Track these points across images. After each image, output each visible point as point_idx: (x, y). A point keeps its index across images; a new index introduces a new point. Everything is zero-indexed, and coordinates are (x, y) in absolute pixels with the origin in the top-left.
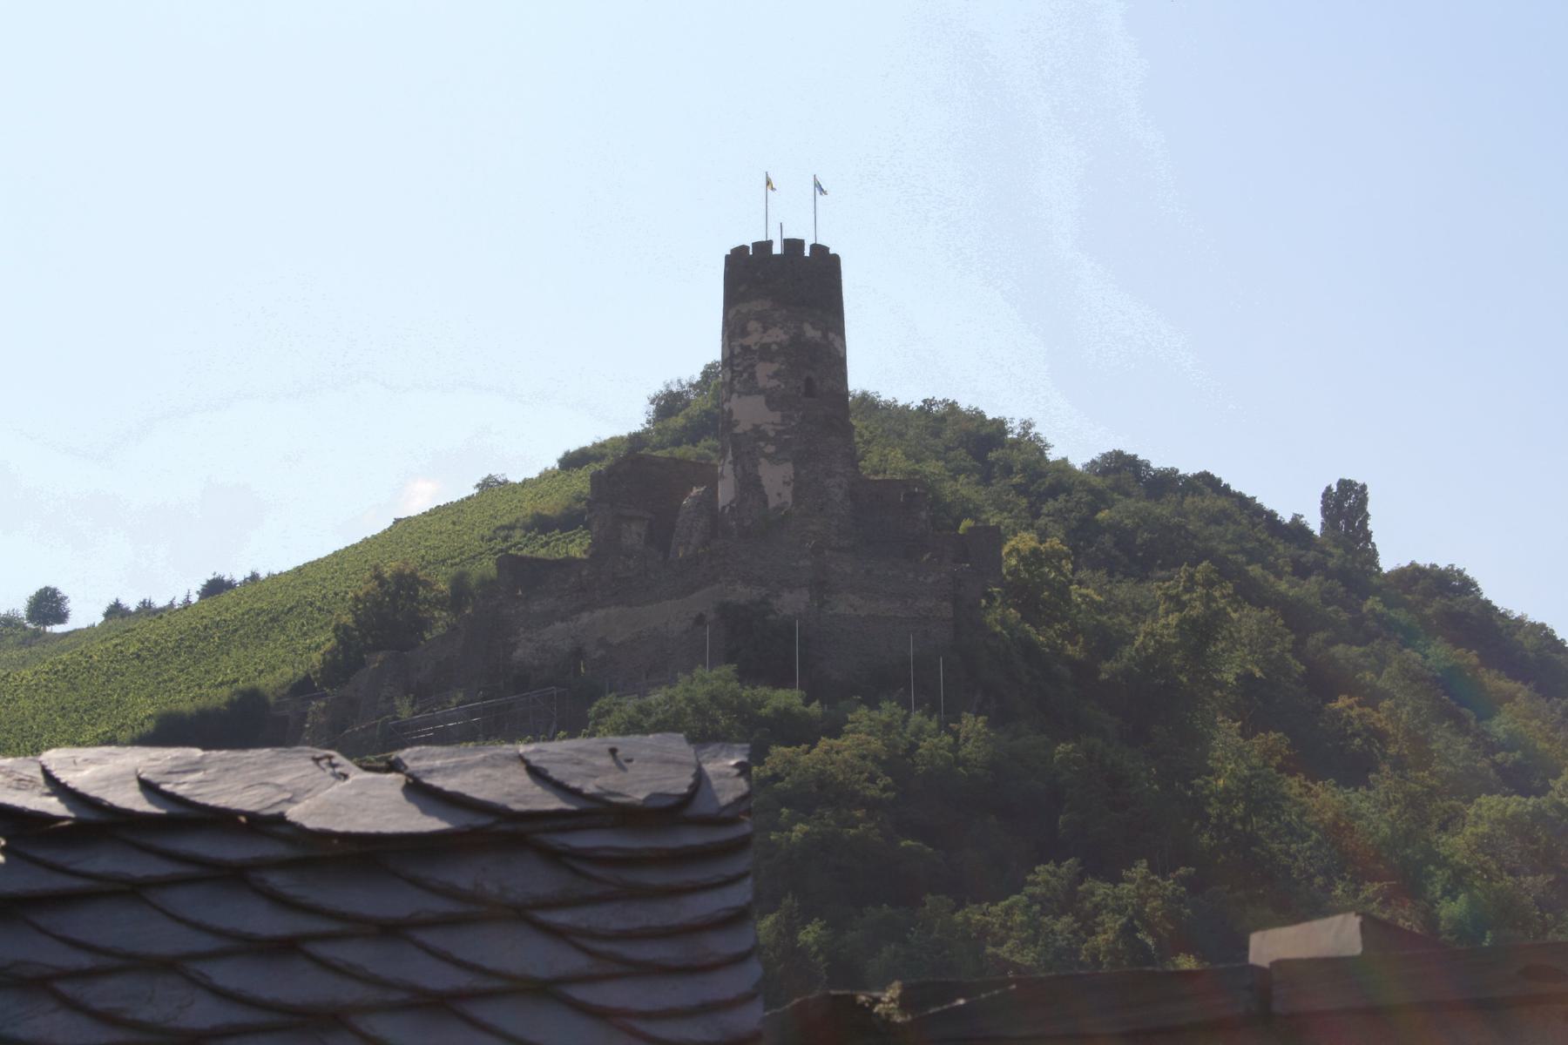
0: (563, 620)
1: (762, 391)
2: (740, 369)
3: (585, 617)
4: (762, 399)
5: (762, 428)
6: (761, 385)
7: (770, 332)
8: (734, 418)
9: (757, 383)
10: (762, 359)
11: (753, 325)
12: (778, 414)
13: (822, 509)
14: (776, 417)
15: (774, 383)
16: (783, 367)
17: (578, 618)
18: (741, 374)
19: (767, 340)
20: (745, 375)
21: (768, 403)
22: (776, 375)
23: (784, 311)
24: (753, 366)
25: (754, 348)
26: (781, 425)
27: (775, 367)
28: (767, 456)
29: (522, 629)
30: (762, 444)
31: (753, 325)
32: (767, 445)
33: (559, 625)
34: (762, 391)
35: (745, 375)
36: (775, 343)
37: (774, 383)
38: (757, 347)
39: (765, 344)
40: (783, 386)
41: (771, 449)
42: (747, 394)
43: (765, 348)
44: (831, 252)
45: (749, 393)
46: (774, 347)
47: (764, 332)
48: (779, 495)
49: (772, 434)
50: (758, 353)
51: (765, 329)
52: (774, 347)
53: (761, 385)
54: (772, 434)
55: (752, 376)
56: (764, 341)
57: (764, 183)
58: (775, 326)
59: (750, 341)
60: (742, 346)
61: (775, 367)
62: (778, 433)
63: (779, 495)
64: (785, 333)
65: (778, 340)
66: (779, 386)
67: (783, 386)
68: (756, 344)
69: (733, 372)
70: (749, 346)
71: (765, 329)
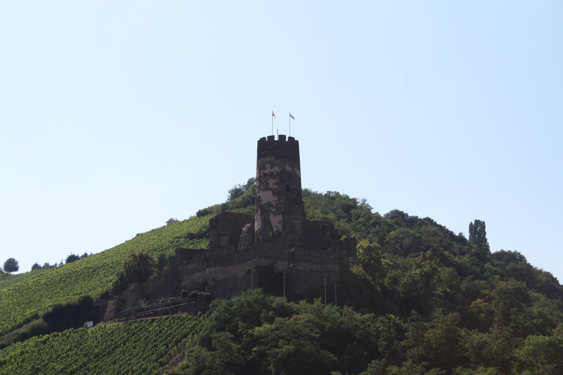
0: (200, 271)
2: (263, 181)
3: (208, 271)
5: (271, 202)
6: (270, 187)
7: (273, 168)
10: (271, 178)
11: (268, 166)
14: (276, 198)
15: (275, 186)
16: (278, 181)
18: (263, 183)
19: (272, 171)
20: (265, 184)
22: (276, 183)
23: (279, 161)
24: (267, 180)
25: (268, 174)
26: (278, 201)
27: (276, 181)
28: (273, 213)
30: (271, 208)
31: (268, 166)
32: (272, 209)
33: (198, 274)
34: (270, 189)
35: (265, 184)
36: (275, 172)
37: (275, 186)
38: (269, 174)
41: (274, 210)
44: (295, 139)
45: (266, 190)
46: (275, 174)
47: (272, 168)
48: (277, 226)
49: (274, 205)
50: (269, 176)
52: (275, 174)
53: (270, 187)
54: (274, 205)
55: (267, 184)
56: (271, 171)
57: (272, 115)
59: (266, 171)
60: (263, 173)
61: (276, 181)
63: (277, 226)
64: (279, 168)
65: (277, 171)
66: (277, 187)
67: (278, 188)
68: (269, 172)
69: (260, 182)
71: (272, 167)
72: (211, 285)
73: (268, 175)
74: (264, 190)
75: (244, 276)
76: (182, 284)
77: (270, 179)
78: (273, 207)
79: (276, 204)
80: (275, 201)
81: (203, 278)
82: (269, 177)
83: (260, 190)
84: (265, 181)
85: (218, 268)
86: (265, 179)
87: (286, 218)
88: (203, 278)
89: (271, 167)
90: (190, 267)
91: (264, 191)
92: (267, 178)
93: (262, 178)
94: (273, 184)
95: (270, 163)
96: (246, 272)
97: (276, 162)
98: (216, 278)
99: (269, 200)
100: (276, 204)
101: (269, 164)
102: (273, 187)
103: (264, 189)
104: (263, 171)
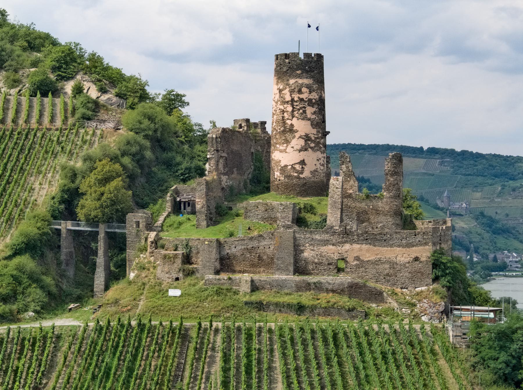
0: (333, 245)
1: (309, 119)
2: (298, 107)
3: (347, 246)
4: (309, 123)
6: (309, 116)
7: (312, 94)
8: (295, 128)
10: (309, 105)
11: (304, 90)
12: (316, 130)
13: (399, 196)
14: (314, 131)
15: (313, 117)
16: (317, 110)
17: (343, 246)
18: (299, 110)
19: (311, 97)
20: (301, 111)
21: (312, 125)
22: (314, 113)
23: (317, 85)
25: (305, 100)
26: (317, 135)
27: (314, 109)
28: (311, 148)
29: (307, 245)
30: (309, 142)
31: (304, 90)
33: (331, 247)
34: (309, 119)
35: (301, 111)
36: (314, 99)
38: (307, 100)
39: (310, 99)
40: (317, 118)
41: (313, 145)
42: (302, 119)
43: (310, 100)
46: (314, 101)
47: (310, 94)
48: (315, 165)
50: (307, 102)
51: (310, 92)
52: (314, 101)
53: (309, 116)
54: (313, 139)
55: (305, 112)
56: (309, 97)
57: (307, 26)
59: (301, 96)
60: (299, 98)
61: (314, 109)
62: (316, 138)
63: (315, 165)
64: (318, 95)
65: (315, 98)
67: (317, 118)
69: (293, 108)
70: (303, 98)
71: (310, 92)
72: (352, 264)
73: (306, 102)
74: (299, 118)
75: (409, 262)
76: (302, 254)
78: (312, 141)
79: (315, 138)
80: (313, 134)
82: (306, 104)
83: (293, 117)
84: (301, 108)
85: (364, 247)
86: (301, 106)
87: (392, 179)
88: (340, 254)
90: (317, 237)
91: (300, 120)
92: (305, 105)
93: (298, 104)
95: (308, 87)
96: (412, 259)
97: (315, 86)
98: (361, 257)
99: (307, 133)
100: (315, 138)
101: (306, 87)
102: (312, 118)
103: (300, 117)
104: (298, 95)
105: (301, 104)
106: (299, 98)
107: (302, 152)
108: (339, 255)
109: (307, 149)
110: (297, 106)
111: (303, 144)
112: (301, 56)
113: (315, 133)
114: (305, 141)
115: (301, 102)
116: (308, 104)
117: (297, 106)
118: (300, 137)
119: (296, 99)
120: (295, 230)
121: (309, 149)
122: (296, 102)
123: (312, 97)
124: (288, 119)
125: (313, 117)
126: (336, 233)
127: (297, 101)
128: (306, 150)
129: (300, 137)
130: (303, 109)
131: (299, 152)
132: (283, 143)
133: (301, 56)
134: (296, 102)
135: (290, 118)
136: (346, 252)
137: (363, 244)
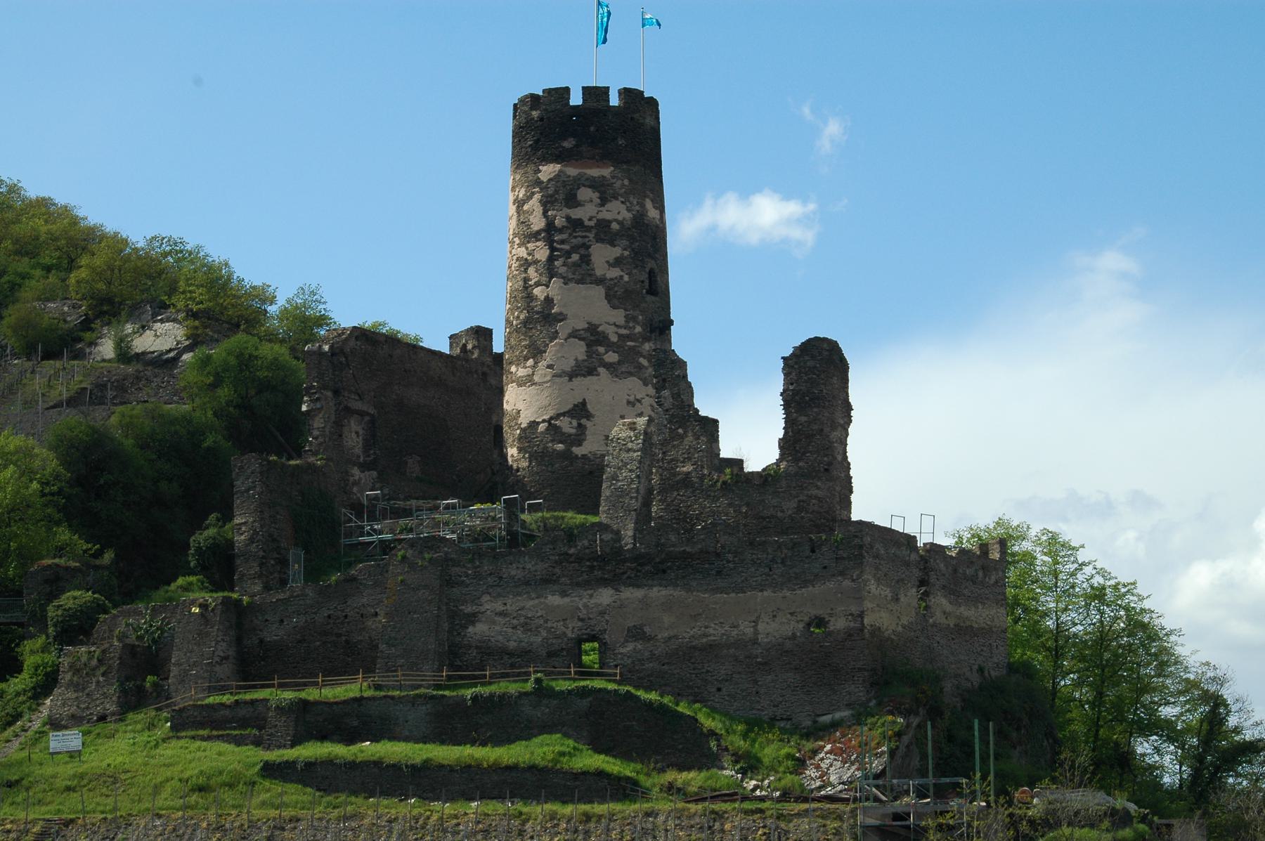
1: (600, 281)
2: (566, 247)
5: (600, 329)
7: (608, 206)
9: (593, 270)
10: (599, 239)
15: (614, 273)
16: (626, 253)
18: (568, 254)
20: (575, 257)
21: (609, 297)
22: (617, 262)
25: (587, 223)
28: (608, 366)
30: (601, 349)
31: (584, 194)
34: (600, 281)
38: (592, 223)
41: (612, 357)
42: (578, 282)
54: (614, 339)
55: (586, 259)
58: (617, 199)
59: (576, 213)
60: (568, 218)
64: (628, 210)
65: (620, 218)
66: (621, 277)
67: (626, 278)
71: (604, 201)
73: (589, 229)
74: (571, 280)
76: (471, 629)
77: (599, 245)
78: (610, 346)
79: (620, 336)
80: (615, 324)
81: (582, 620)
88: (582, 620)
89: (599, 201)
91: (572, 285)
94: (608, 262)
103: (571, 276)
104: (566, 211)
105: (576, 237)
106: (568, 218)
107: (579, 379)
108: (580, 624)
109: (595, 369)
110: (562, 242)
111: (582, 357)
112: (576, 99)
113: (621, 321)
114: (588, 345)
115: (574, 231)
116: (596, 234)
117: (562, 242)
118: (574, 334)
119: (559, 222)
120: (446, 553)
121: (601, 370)
122: (561, 231)
123: (608, 216)
124: (538, 284)
125: (614, 273)
126: (571, 555)
127: (563, 227)
128: (591, 372)
129: (574, 334)
130: (582, 251)
131: (570, 380)
132: (526, 359)
133: (576, 99)
134: (561, 231)
135: (544, 279)
136: (602, 613)
137: (651, 587)
